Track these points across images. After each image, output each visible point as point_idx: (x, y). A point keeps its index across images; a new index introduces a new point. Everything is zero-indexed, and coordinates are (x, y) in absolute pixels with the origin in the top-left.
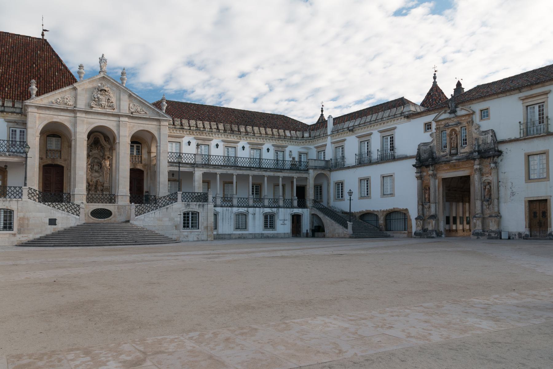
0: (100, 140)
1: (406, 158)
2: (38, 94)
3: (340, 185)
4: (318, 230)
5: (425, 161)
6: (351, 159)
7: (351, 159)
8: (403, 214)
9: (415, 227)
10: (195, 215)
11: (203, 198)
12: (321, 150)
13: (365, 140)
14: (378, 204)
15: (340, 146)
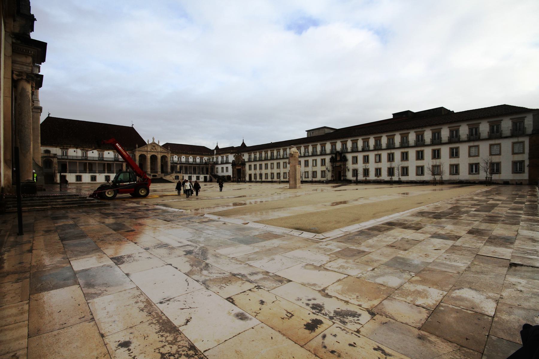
0: (154, 158)
1: (230, 163)
2: (138, 147)
3: (217, 168)
4: (211, 181)
5: (234, 164)
6: (220, 162)
7: (220, 162)
8: (230, 176)
9: (232, 180)
10: (178, 176)
11: (180, 172)
12: (213, 158)
13: (222, 158)
14: (225, 174)
15: (217, 158)
